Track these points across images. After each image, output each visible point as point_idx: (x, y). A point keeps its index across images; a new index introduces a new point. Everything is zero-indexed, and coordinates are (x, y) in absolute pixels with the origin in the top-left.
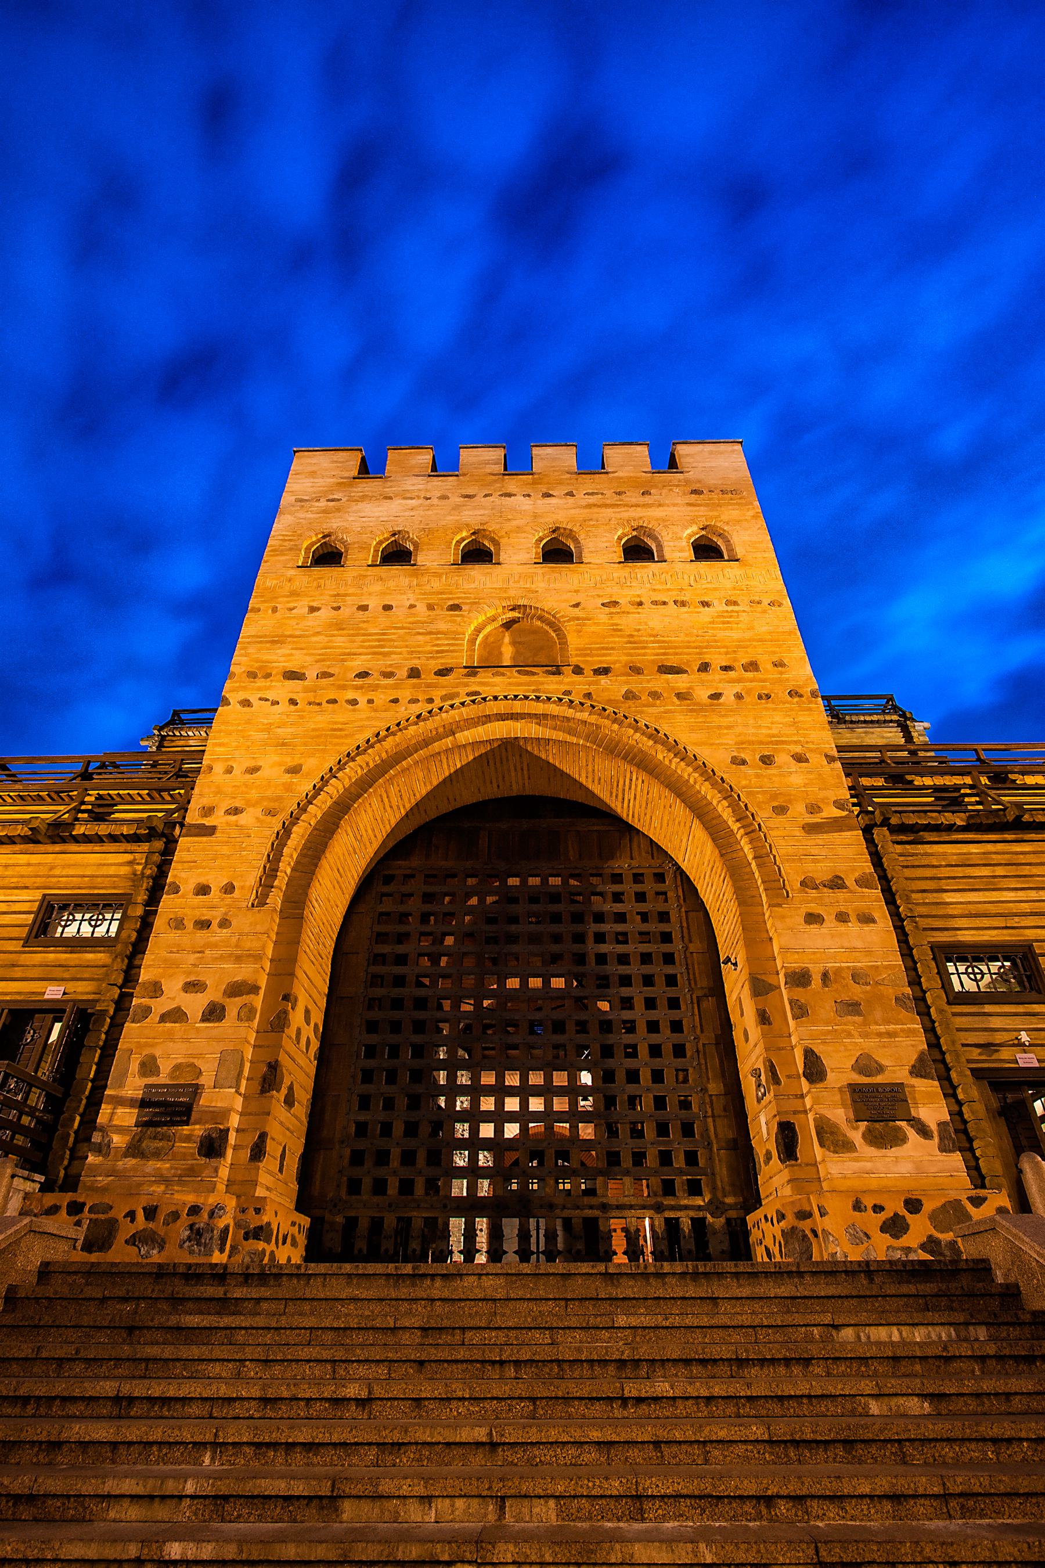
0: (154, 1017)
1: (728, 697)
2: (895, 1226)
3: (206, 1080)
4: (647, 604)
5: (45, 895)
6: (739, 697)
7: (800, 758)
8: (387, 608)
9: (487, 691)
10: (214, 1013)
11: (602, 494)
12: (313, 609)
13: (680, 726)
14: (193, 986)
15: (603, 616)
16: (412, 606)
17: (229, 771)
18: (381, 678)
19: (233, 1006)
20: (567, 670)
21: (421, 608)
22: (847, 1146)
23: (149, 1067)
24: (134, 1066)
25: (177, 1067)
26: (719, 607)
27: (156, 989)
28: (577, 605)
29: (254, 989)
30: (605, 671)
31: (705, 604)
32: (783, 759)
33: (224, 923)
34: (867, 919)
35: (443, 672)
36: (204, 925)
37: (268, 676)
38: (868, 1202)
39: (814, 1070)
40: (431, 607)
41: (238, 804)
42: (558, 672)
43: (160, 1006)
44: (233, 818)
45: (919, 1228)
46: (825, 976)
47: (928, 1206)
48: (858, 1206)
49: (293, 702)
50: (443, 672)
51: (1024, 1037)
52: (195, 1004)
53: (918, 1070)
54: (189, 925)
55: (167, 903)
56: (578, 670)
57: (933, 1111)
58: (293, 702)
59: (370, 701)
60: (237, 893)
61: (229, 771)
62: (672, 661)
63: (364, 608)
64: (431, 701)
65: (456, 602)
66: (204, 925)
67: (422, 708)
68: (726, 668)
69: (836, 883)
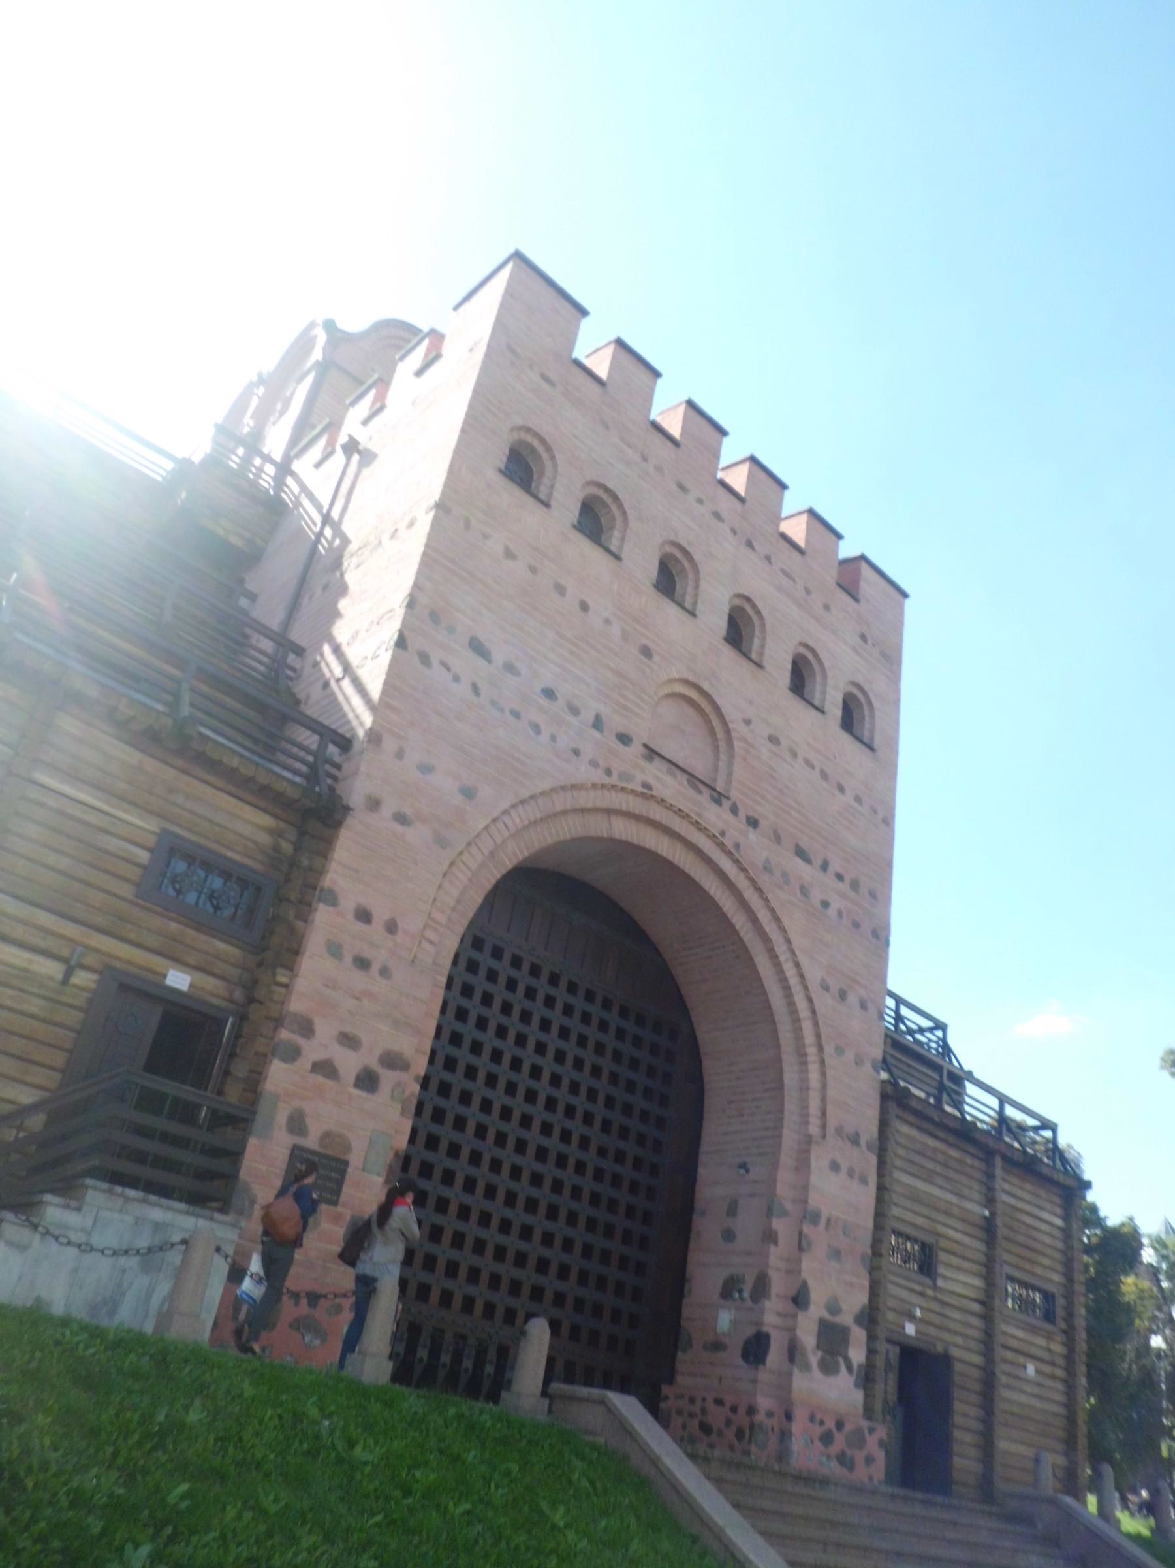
0: (305, 1062)
1: (832, 912)
2: (827, 1438)
3: (355, 1159)
4: (800, 760)
5: (165, 832)
6: (840, 914)
7: (863, 1006)
8: (584, 607)
9: (659, 790)
10: (367, 1081)
11: (794, 581)
12: (509, 554)
13: (795, 922)
14: (349, 1040)
15: (765, 750)
16: (607, 622)
17: (400, 755)
18: (567, 710)
19: (388, 1079)
20: (726, 804)
21: (616, 630)
22: (807, 1367)
23: (297, 1124)
24: (282, 1117)
25: (327, 1136)
26: (848, 798)
27: (306, 1028)
28: (748, 722)
29: (405, 1066)
30: (753, 823)
31: (841, 789)
32: (852, 998)
33: (385, 972)
34: (864, 1181)
35: (624, 739)
36: (362, 964)
37: (451, 629)
38: (818, 1417)
39: (800, 1299)
40: (625, 636)
41: (408, 811)
42: (718, 802)
43: (313, 1051)
44: (399, 828)
45: (840, 1441)
46: (829, 1221)
47: (848, 1428)
48: (812, 1419)
49: (475, 689)
50: (624, 739)
51: (918, 1313)
52: (349, 1063)
53: (858, 1320)
54: (348, 959)
55: (322, 914)
56: (734, 810)
57: (857, 1355)
58: (475, 689)
59: (553, 738)
60: (399, 937)
61: (400, 755)
62: (805, 844)
63: (560, 590)
64: (609, 772)
65: (650, 645)
66: (362, 964)
67: (598, 776)
68: (839, 877)
69: (855, 1140)
